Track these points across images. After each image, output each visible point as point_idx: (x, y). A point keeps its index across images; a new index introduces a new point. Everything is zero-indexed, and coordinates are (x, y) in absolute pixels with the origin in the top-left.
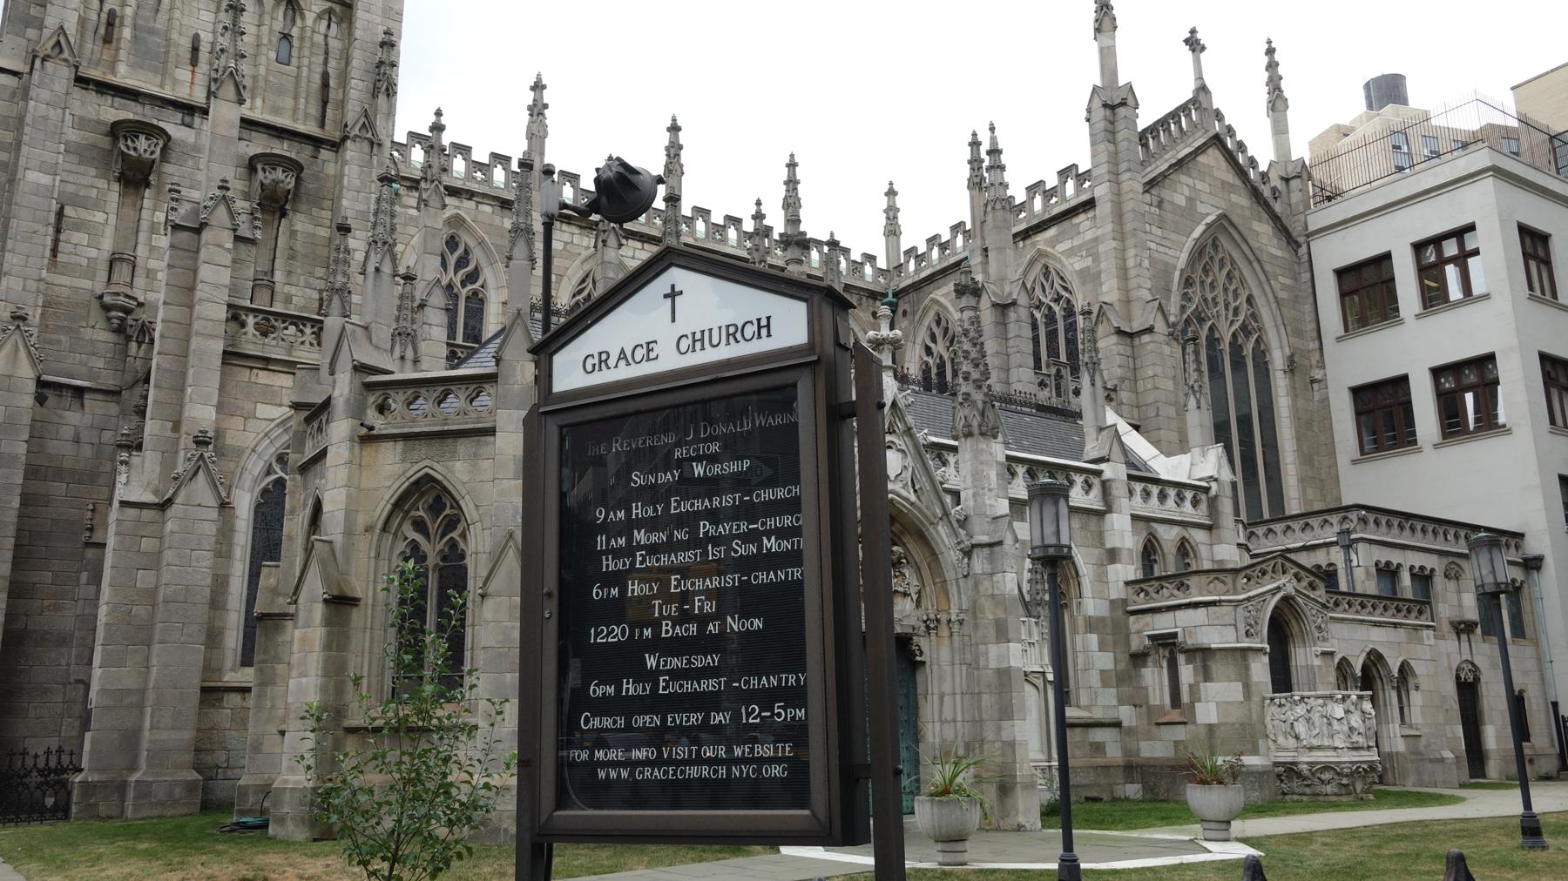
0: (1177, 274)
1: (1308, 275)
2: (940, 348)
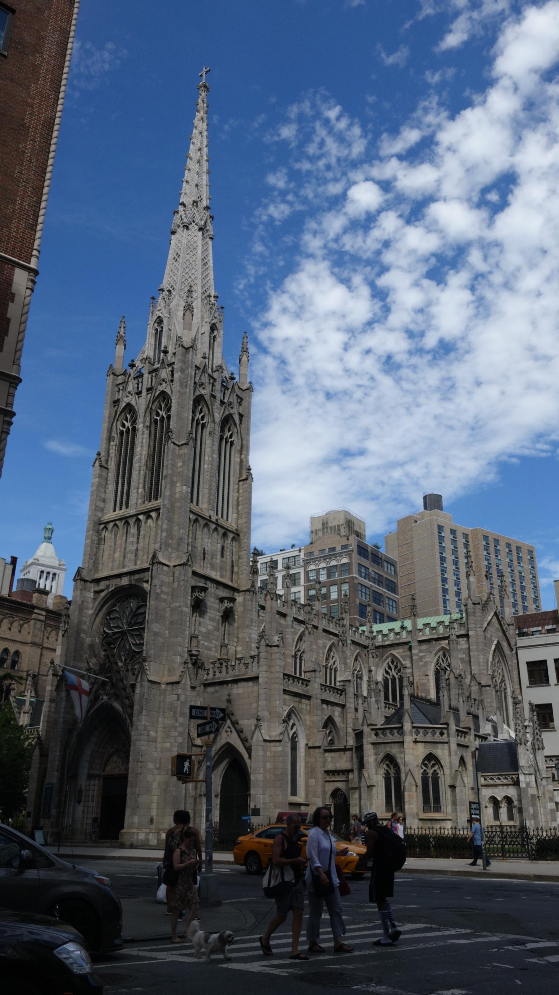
0: (490, 663)
1: (515, 661)
2: (393, 672)
